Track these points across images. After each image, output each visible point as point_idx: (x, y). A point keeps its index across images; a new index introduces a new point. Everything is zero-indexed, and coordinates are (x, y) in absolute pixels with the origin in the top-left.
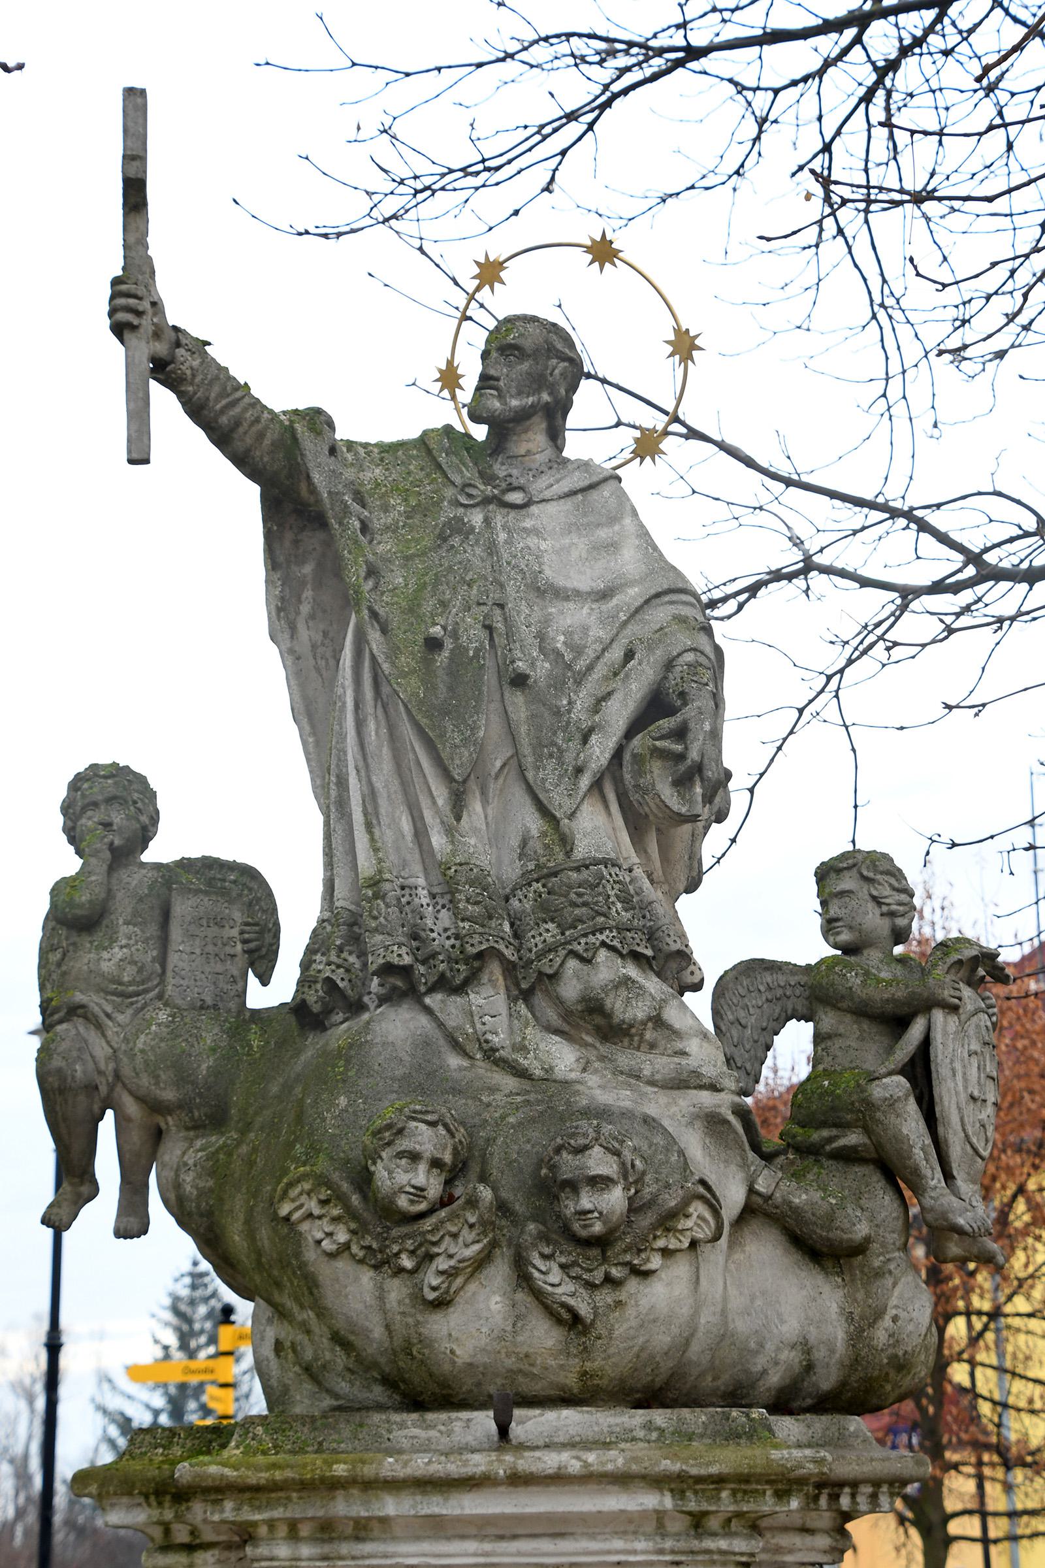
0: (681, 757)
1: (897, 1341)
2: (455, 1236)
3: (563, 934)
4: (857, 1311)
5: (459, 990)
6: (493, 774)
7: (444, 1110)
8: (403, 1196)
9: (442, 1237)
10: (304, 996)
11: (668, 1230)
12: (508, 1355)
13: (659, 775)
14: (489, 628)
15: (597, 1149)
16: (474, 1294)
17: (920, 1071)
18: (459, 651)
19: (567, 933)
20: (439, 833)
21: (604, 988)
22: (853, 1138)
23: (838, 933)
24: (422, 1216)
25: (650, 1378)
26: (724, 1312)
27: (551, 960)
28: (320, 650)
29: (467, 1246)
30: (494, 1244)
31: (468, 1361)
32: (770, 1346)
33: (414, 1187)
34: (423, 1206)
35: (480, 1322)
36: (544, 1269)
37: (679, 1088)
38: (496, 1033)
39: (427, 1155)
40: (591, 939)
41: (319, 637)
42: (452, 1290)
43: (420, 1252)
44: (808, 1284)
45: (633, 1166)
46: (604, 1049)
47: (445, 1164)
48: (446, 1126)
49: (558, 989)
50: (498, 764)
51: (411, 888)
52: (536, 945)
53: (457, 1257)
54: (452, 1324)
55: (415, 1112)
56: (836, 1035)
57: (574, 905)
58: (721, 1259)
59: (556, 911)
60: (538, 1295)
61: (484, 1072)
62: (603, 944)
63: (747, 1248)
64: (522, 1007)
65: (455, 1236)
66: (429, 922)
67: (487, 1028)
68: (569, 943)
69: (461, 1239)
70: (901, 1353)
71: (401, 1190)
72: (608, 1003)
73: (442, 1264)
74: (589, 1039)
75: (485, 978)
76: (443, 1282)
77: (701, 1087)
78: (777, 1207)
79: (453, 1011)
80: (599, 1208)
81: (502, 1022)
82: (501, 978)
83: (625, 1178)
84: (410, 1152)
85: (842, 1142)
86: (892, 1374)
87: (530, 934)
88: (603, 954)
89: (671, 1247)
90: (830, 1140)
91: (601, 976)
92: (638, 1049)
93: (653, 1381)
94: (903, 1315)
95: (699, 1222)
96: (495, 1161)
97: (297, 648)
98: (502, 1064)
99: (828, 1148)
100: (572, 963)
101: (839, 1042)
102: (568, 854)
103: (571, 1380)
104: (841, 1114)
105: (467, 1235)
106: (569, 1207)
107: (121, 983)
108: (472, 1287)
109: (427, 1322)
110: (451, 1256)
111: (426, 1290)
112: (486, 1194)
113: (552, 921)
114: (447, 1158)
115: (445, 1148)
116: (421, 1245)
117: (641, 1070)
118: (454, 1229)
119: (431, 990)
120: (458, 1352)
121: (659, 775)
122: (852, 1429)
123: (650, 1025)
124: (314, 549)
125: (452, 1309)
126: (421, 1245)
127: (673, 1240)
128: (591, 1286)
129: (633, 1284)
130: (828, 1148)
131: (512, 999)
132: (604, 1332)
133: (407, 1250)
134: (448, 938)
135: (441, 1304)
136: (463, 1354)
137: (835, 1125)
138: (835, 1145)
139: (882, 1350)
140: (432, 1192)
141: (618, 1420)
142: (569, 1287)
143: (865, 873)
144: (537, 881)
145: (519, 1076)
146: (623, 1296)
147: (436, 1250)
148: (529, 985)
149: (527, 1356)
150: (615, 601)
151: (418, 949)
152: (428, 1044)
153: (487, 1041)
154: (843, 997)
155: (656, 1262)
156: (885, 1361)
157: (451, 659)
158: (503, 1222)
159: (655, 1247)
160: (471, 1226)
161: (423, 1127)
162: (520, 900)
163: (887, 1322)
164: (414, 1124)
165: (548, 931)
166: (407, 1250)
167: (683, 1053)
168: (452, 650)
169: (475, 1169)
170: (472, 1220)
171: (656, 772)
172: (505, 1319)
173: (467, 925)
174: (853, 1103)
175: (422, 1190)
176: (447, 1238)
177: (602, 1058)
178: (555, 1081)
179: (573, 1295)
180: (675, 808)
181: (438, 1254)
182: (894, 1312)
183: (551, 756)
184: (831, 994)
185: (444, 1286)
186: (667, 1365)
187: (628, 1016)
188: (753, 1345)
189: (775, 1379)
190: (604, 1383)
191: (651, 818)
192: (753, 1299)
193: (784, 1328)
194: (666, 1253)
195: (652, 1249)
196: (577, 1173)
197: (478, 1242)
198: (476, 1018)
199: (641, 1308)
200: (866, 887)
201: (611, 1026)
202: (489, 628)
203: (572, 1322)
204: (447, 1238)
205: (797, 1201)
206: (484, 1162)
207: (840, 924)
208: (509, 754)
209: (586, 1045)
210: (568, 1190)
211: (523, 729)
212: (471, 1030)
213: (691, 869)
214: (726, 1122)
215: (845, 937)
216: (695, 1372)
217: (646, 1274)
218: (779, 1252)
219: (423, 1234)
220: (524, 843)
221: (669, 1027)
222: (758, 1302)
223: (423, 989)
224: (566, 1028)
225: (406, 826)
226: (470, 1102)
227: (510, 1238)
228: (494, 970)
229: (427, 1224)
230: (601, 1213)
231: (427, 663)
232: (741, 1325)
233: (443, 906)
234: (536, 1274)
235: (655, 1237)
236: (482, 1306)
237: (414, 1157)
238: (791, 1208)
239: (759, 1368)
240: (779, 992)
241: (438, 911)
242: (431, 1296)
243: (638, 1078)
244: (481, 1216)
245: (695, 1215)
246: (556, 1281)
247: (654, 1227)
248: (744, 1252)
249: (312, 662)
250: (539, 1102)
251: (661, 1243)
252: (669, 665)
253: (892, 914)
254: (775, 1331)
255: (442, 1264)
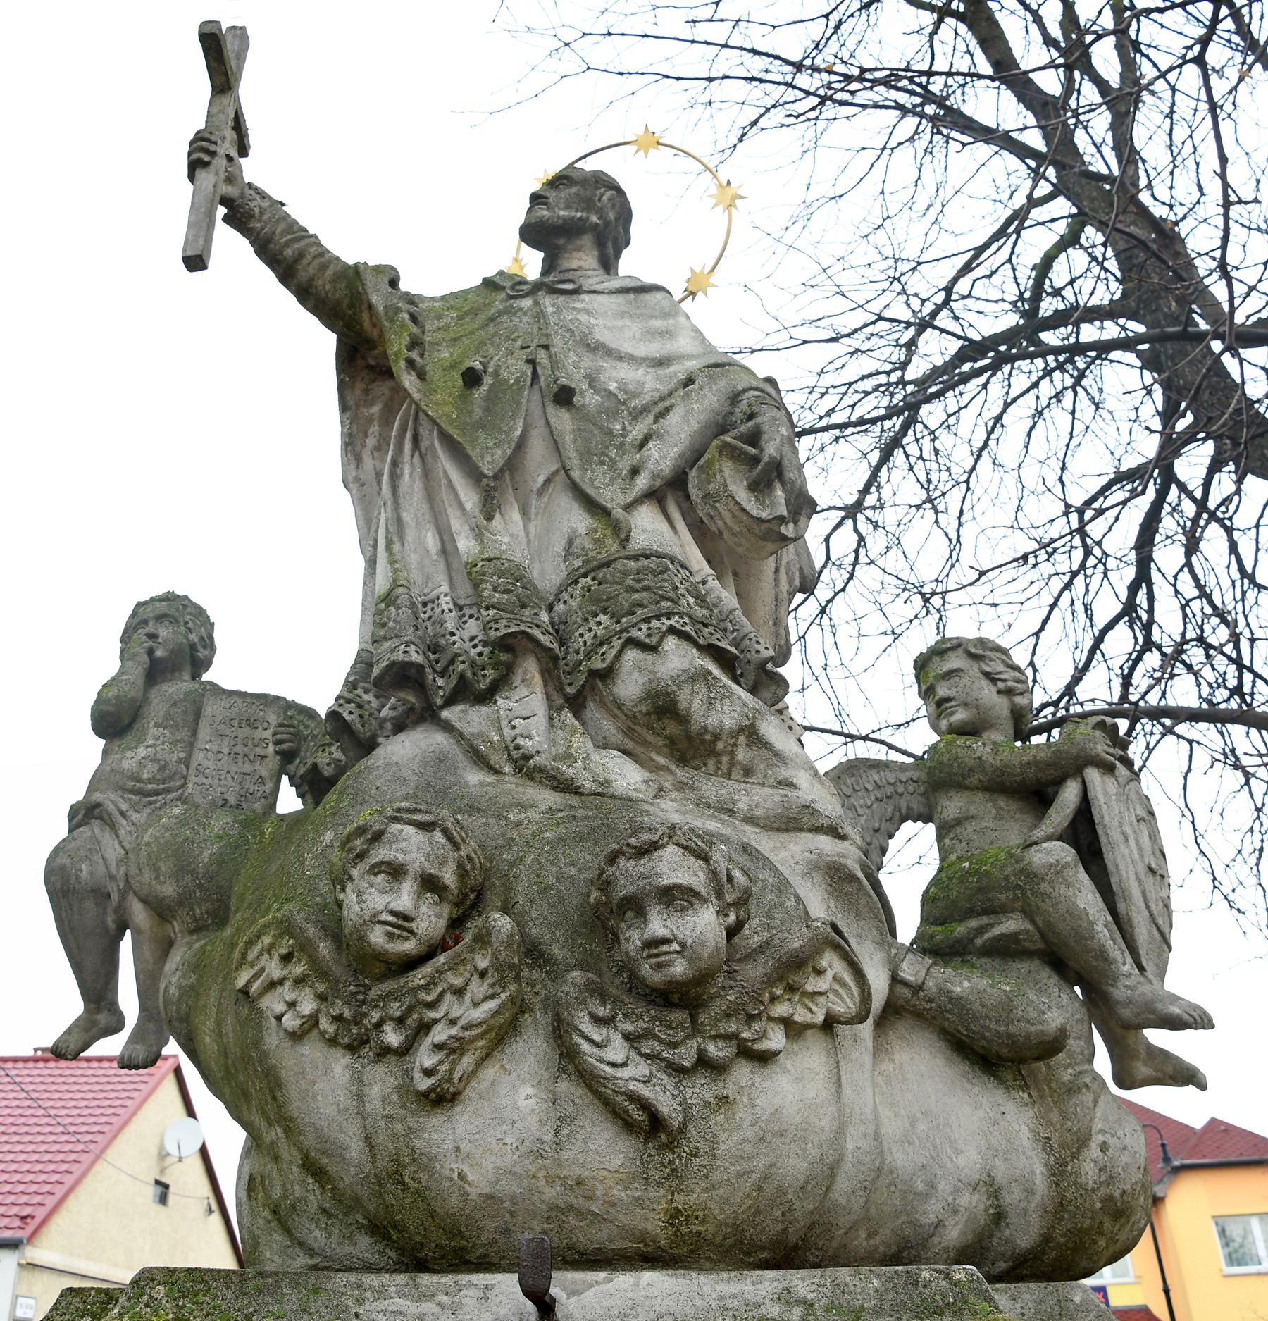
0: (755, 460)
1: (1111, 1177)
2: (459, 992)
4: (1055, 1137)
5: (487, 697)
6: (535, 489)
7: (444, 813)
8: (378, 928)
9: (442, 994)
11: (791, 989)
12: (550, 1181)
13: (731, 477)
14: (532, 362)
15: (671, 848)
16: (492, 1084)
17: (1084, 835)
18: (499, 383)
19: (624, 620)
20: (467, 537)
21: (675, 679)
22: (1010, 925)
23: (952, 714)
24: (411, 963)
25: (780, 1227)
26: (877, 1136)
27: (603, 654)
29: (476, 1005)
30: (519, 1007)
31: (487, 1191)
32: (944, 1187)
33: (393, 913)
34: (409, 946)
35: (505, 1129)
36: (597, 1038)
37: (788, 830)
38: (529, 737)
39: (414, 868)
40: (655, 624)
42: (456, 1076)
43: (412, 1020)
44: (984, 1101)
45: (730, 879)
46: (682, 774)
47: (445, 888)
48: (446, 832)
49: (615, 690)
50: (541, 479)
51: (433, 601)
52: (585, 643)
53: (461, 1022)
54: (460, 1131)
55: (399, 810)
56: (967, 819)
57: (632, 590)
58: (867, 1059)
59: (608, 599)
60: (590, 1081)
61: (514, 787)
62: (672, 631)
63: (897, 1056)
64: (568, 717)
65: (459, 992)
66: (450, 626)
67: (517, 731)
68: (627, 630)
69: (468, 996)
70: (1117, 1194)
71: (375, 919)
72: (683, 698)
73: (440, 1034)
74: (661, 760)
75: (517, 680)
76: (440, 1063)
77: (818, 830)
78: (931, 1000)
79: (476, 719)
80: (680, 937)
81: (538, 725)
82: (538, 677)
83: (719, 894)
84: (389, 863)
85: (997, 931)
86: (1107, 1224)
87: (577, 634)
88: (671, 643)
89: (797, 1018)
90: (980, 931)
91: (670, 665)
92: (728, 775)
93: (785, 1231)
94: (1112, 1142)
95: (837, 987)
96: (522, 885)
98: (538, 776)
99: (979, 942)
100: (632, 655)
101: (971, 827)
102: (624, 542)
103: (654, 1223)
104: (992, 895)
105: (478, 988)
106: (633, 939)
108: (490, 1073)
109: (423, 1129)
110: (453, 1022)
111: (417, 1075)
112: (502, 923)
113: (605, 613)
114: (449, 876)
115: (443, 862)
116: (411, 1009)
117: (734, 802)
118: (458, 982)
119: (449, 702)
120: (471, 1177)
121: (731, 477)
122: (1077, 1299)
123: (742, 739)
125: (459, 1109)
126: (411, 1009)
127: (800, 1009)
128: (677, 1071)
129: (743, 1072)
130: (979, 942)
131: (553, 709)
132: (702, 1146)
133: (392, 1019)
134: (475, 646)
135: (440, 1099)
136: (479, 1179)
137: (986, 912)
138: (986, 936)
139: (1093, 1190)
140: (424, 925)
141: (735, 1288)
142: (640, 1068)
143: (973, 650)
145: (562, 790)
146: (730, 1091)
147: (433, 1015)
148: (579, 691)
149: (579, 1183)
150: (672, 369)
151: (437, 662)
152: (441, 761)
153: (517, 748)
154: (971, 770)
155: (776, 1039)
156: (1098, 1205)
157: (490, 391)
158: (536, 975)
159: (774, 1014)
160: (483, 974)
161: (411, 830)
162: (565, 602)
163: (1093, 1151)
164: (396, 827)
165: (599, 623)
166: (392, 1019)
167: (792, 785)
168: (491, 385)
169: (493, 899)
170: (483, 964)
171: (727, 473)
172: (542, 1123)
173: (491, 612)
174: (1007, 878)
175: (407, 918)
176: (448, 996)
177: (681, 787)
178: (613, 797)
179: (647, 1081)
180: (755, 513)
181: (436, 1021)
182: (1101, 1138)
183: (602, 463)
184: (956, 769)
185: (443, 1068)
186: (804, 1207)
187: (712, 721)
188: (920, 1186)
189: (954, 1234)
190: (708, 1229)
191: (726, 535)
192: (913, 1122)
193: (961, 1161)
194: (787, 1023)
195: (770, 1019)
196: (641, 883)
197: (492, 997)
198: (504, 723)
199: (759, 1111)
200: (975, 666)
201: (689, 737)
202: (532, 362)
203: (649, 1126)
204: (448, 996)
205: (958, 989)
206: (507, 888)
207: (953, 703)
208: (555, 467)
209: (657, 768)
210: (630, 914)
211: (568, 438)
212: (497, 738)
213: (777, 635)
214: (855, 879)
215: (960, 716)
216: (844, 1222)
217: (765, 1059)
218: (940, 1061)
219: (414, 991)
220: (570, 542)
221: (768, 746)
222: (922, 1126)
223: (439, 701)
224: (630, 745)
225: (431, 541)
226: (492, 821)
227: (547, 997)
228: (530, 668)
229: (418, 977)
230: (683, 945)
231: (464, 397)
232: (902, 1159)
233: (471, 617)
234: (585, 1047)
235: (773, 999)
236: (504, 1102)
237: (396, 871)
238: (951, 999)
239: (931, 1218)
240: (889, 790)
241: (465, 622)
242: (424, 1084)
243: (731, 812)
244: (495, 956)
245: (830, 974)
246: (619, 1057)
247: (770, 981)
248: (893, 1061)
250: (588, 818)
251: (782, 1009)
252: (734, 398)
253: (1009, 692)
254: (949, 1165)
255: (440, 1034)
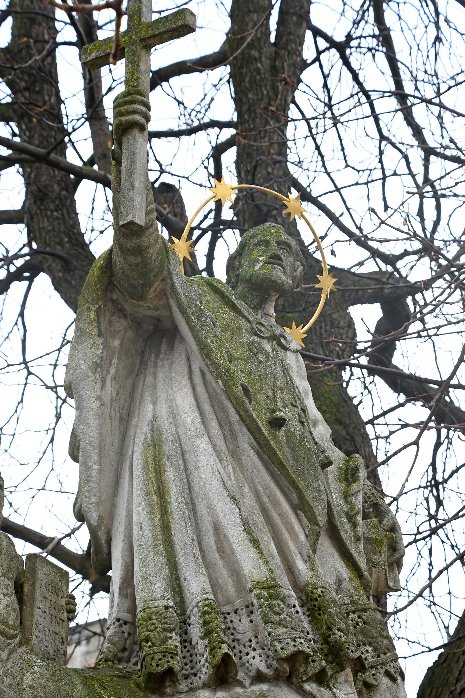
3: (378, 656)
10: (171, 664)
27: (374, 675)
28: (114, 403)
41: (114, 394)
59: (373, 638)
97: (103, 397)
107: (7, 625)
113: (370, 646)
124: (120, 331)
144: (354, 613)
165: (367, 651)
249: (109, 410)
